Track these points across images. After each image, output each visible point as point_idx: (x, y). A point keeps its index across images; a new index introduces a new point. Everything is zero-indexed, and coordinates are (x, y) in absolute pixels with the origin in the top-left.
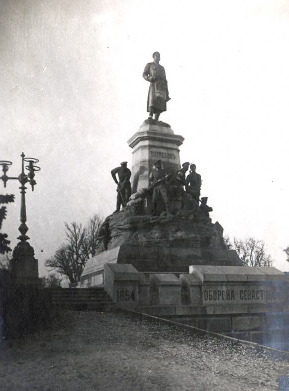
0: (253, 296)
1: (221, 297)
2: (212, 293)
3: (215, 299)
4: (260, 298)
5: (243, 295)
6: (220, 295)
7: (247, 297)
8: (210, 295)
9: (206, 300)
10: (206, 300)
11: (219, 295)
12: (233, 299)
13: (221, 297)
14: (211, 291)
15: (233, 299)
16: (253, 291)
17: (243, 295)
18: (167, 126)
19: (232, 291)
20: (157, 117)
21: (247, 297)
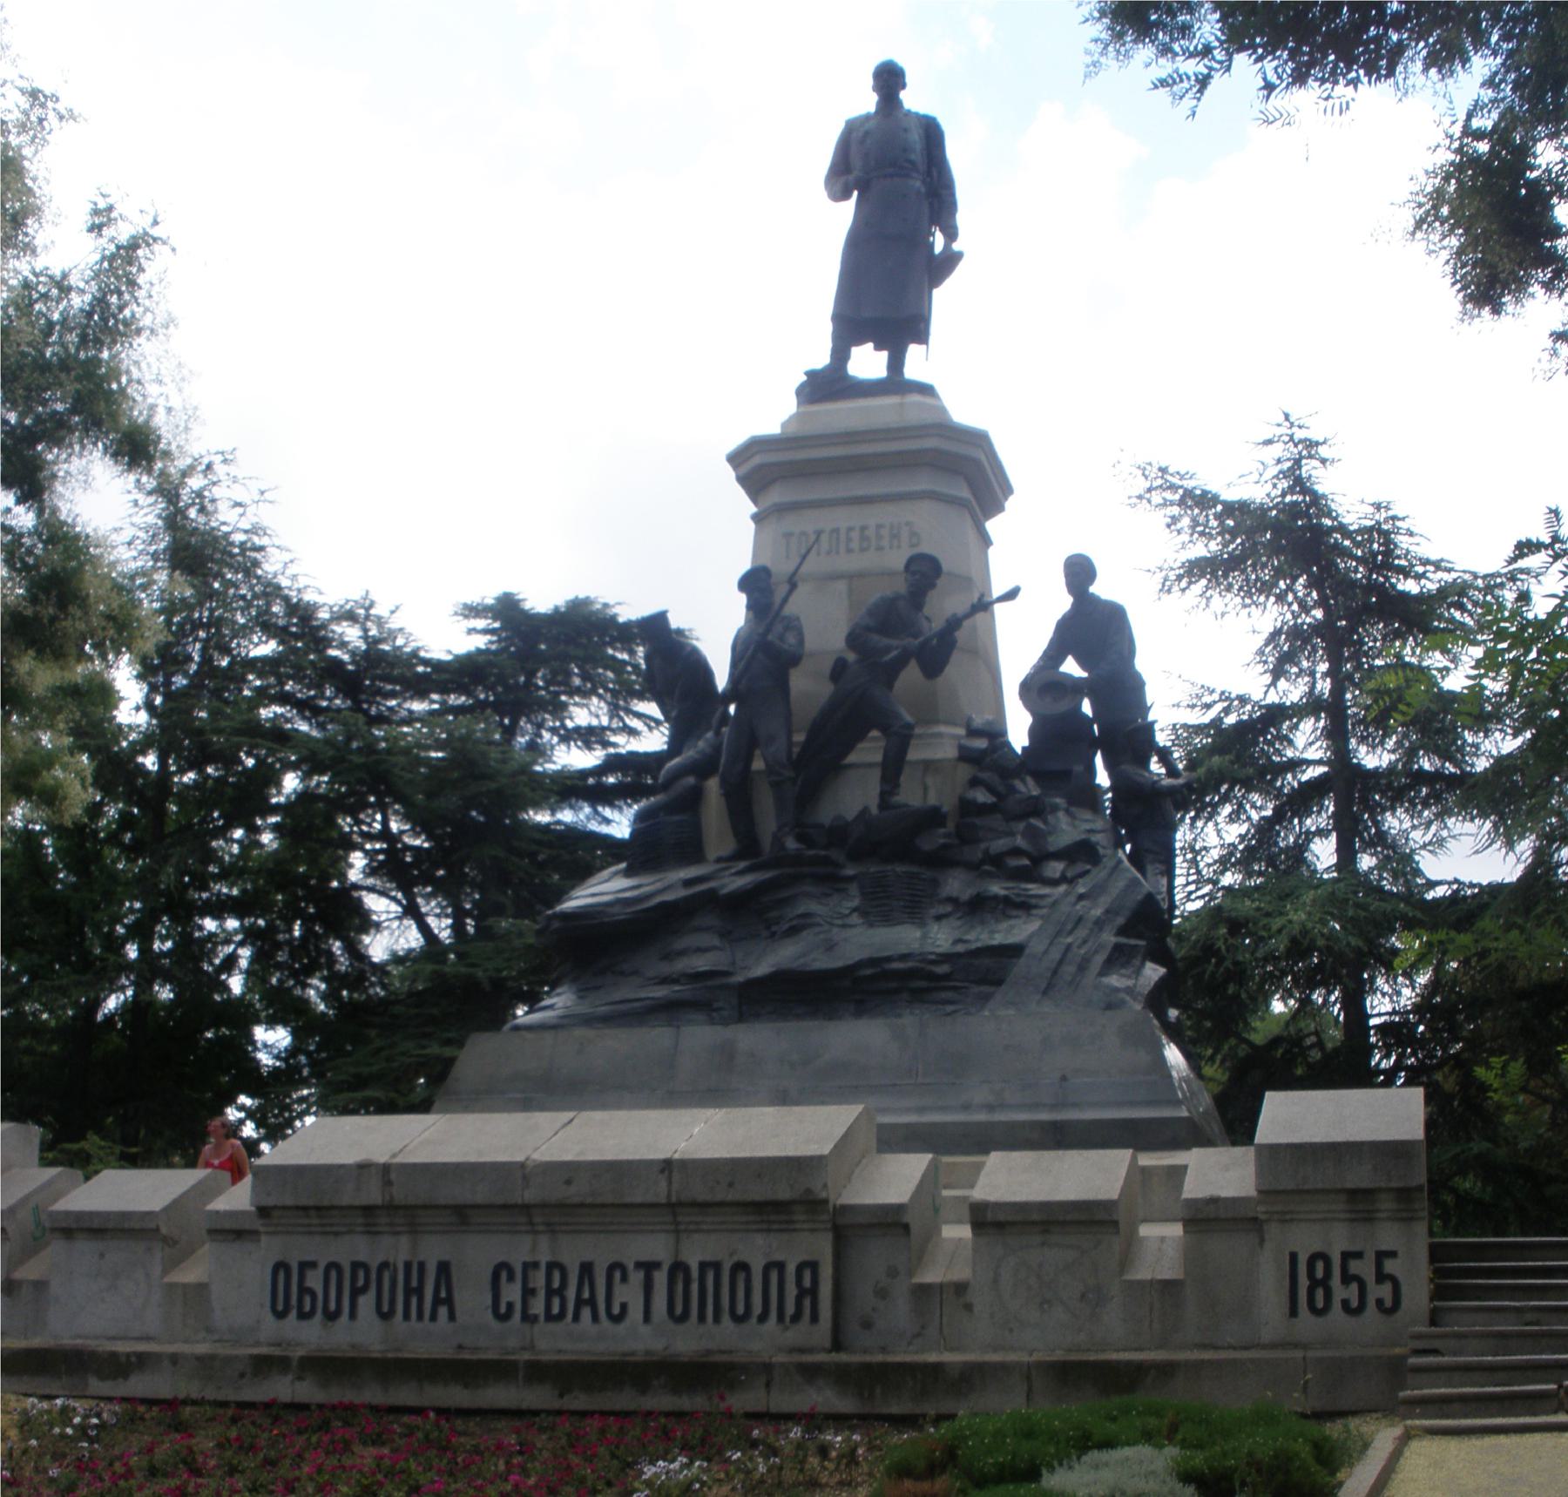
0: (579, 1303)
1: (366, 1302)
2: (314, 1280)
3: (332, 1316)
4: (636, 1312)
5: (512, 1293)
6: (365, 1289)
7: (538, 1306)
8: (304, 1290)
9: (280, 1315)
10: (280, 1315)
11: (356, 1292)
12: (443, 1311)
13: (366, 1302)
14: (313, 1265)
15: (443, 1311)
16: (587, 1269)
17: (512, 1293)
18: (926, 390)
19: (444, 1268)
20: (896, 364)
21: (538, 1306)
